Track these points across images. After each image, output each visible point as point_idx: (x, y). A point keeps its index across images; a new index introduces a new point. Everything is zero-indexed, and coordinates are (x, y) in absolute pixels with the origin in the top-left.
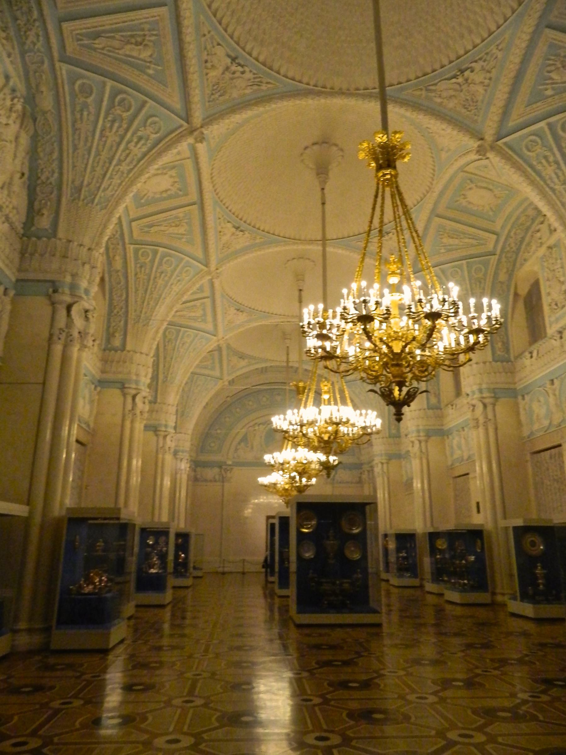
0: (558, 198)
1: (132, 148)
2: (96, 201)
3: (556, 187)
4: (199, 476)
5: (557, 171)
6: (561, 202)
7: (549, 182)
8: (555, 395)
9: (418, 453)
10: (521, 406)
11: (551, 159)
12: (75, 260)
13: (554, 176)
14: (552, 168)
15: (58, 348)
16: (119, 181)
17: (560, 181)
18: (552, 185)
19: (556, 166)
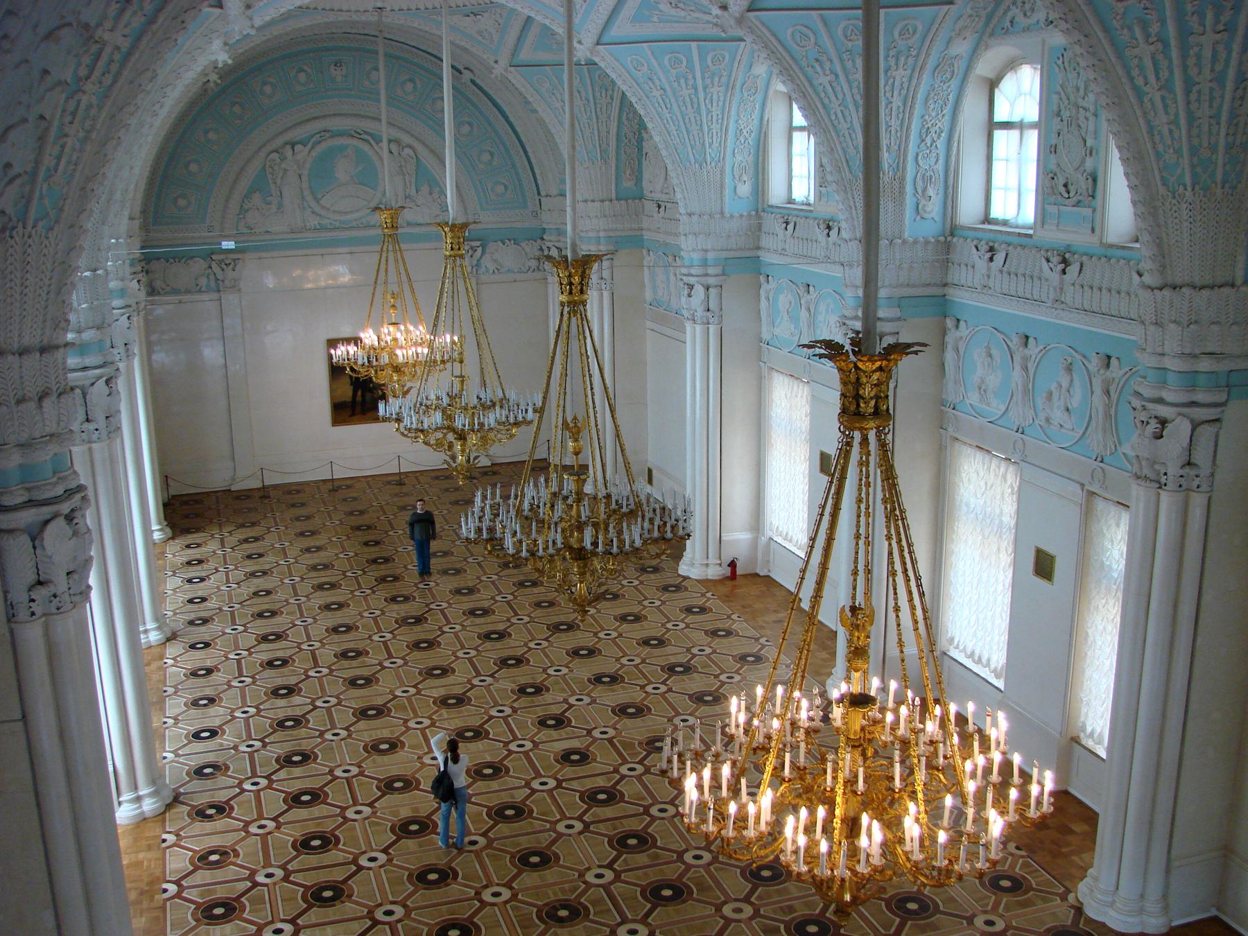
0: (1145, 114)
1: (107, 36)
2: (32, 214)
3: (1146, 89)
4: (158, 284)
5: (1159, 57)
6: (1148, 123)
7: (1135, 73)
8: (1026, 369)
9: (700, 312)
10: (949, 339)
11: (1155, 29)
12: (19, 402)
13: (1148, 63)
14: (1152, 48)
15: (32, 634)
16: (82, 134)
17: (1158, 79)
18: (1140, 82)
19: (1159, 46)
